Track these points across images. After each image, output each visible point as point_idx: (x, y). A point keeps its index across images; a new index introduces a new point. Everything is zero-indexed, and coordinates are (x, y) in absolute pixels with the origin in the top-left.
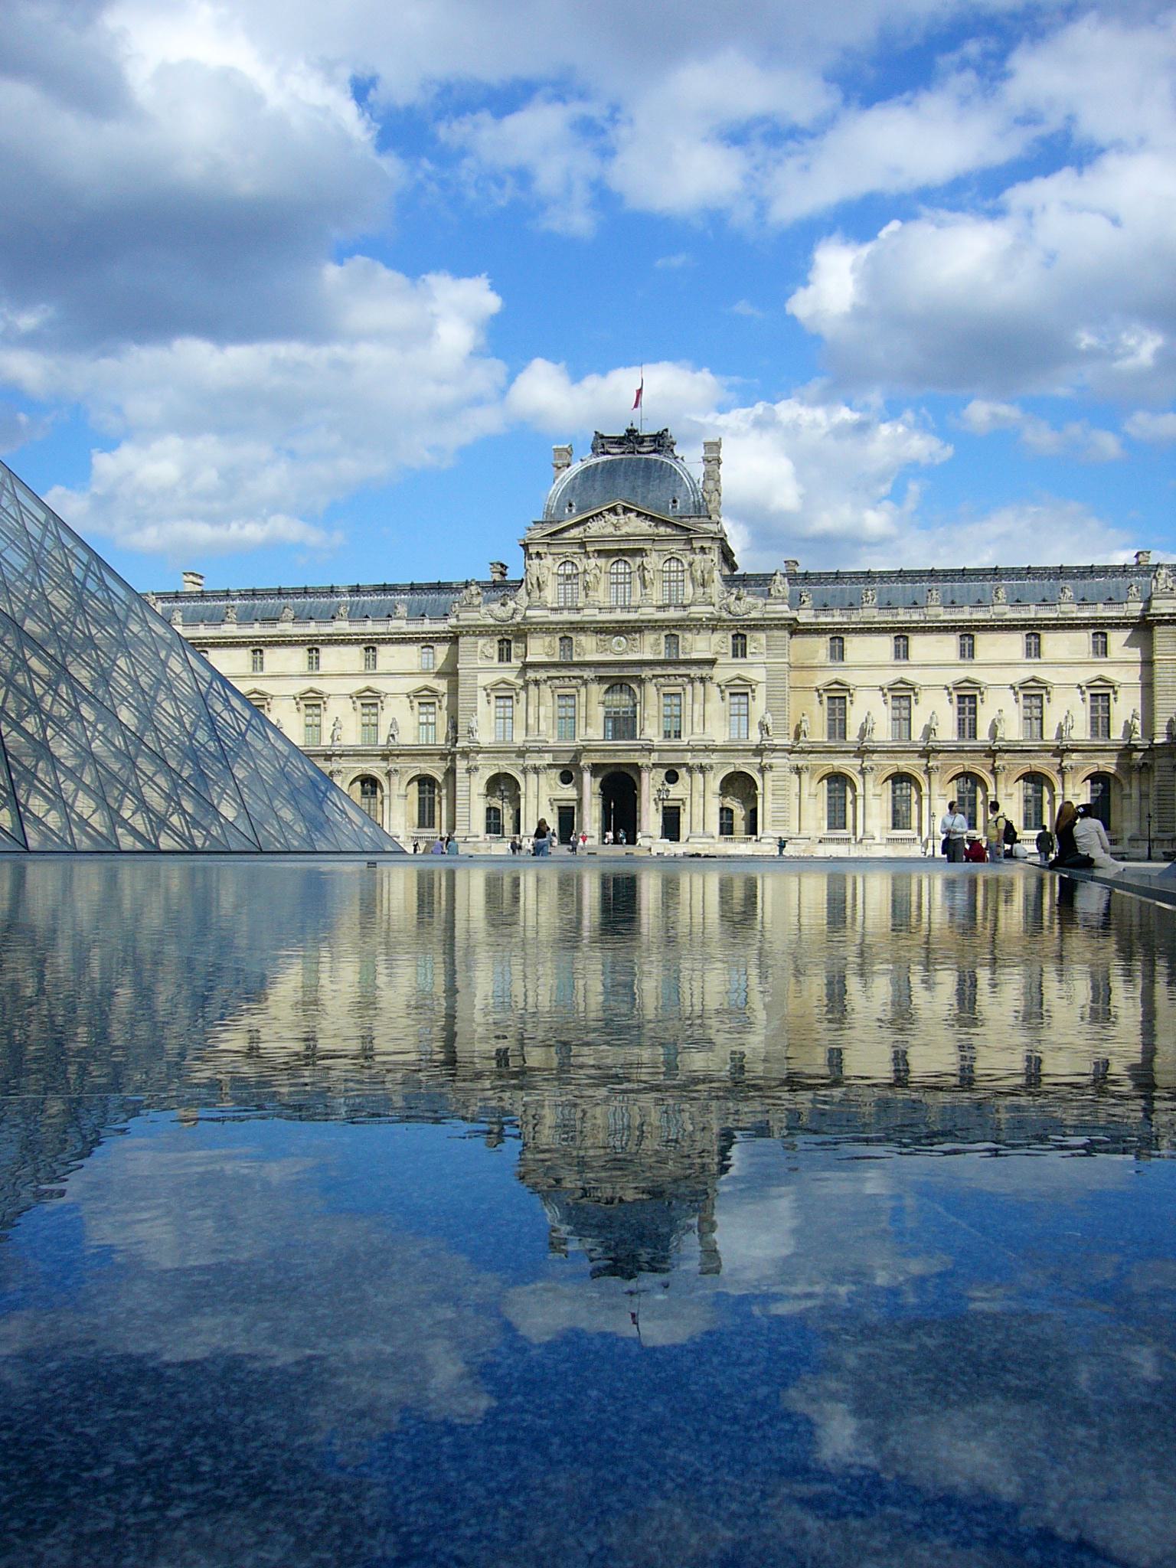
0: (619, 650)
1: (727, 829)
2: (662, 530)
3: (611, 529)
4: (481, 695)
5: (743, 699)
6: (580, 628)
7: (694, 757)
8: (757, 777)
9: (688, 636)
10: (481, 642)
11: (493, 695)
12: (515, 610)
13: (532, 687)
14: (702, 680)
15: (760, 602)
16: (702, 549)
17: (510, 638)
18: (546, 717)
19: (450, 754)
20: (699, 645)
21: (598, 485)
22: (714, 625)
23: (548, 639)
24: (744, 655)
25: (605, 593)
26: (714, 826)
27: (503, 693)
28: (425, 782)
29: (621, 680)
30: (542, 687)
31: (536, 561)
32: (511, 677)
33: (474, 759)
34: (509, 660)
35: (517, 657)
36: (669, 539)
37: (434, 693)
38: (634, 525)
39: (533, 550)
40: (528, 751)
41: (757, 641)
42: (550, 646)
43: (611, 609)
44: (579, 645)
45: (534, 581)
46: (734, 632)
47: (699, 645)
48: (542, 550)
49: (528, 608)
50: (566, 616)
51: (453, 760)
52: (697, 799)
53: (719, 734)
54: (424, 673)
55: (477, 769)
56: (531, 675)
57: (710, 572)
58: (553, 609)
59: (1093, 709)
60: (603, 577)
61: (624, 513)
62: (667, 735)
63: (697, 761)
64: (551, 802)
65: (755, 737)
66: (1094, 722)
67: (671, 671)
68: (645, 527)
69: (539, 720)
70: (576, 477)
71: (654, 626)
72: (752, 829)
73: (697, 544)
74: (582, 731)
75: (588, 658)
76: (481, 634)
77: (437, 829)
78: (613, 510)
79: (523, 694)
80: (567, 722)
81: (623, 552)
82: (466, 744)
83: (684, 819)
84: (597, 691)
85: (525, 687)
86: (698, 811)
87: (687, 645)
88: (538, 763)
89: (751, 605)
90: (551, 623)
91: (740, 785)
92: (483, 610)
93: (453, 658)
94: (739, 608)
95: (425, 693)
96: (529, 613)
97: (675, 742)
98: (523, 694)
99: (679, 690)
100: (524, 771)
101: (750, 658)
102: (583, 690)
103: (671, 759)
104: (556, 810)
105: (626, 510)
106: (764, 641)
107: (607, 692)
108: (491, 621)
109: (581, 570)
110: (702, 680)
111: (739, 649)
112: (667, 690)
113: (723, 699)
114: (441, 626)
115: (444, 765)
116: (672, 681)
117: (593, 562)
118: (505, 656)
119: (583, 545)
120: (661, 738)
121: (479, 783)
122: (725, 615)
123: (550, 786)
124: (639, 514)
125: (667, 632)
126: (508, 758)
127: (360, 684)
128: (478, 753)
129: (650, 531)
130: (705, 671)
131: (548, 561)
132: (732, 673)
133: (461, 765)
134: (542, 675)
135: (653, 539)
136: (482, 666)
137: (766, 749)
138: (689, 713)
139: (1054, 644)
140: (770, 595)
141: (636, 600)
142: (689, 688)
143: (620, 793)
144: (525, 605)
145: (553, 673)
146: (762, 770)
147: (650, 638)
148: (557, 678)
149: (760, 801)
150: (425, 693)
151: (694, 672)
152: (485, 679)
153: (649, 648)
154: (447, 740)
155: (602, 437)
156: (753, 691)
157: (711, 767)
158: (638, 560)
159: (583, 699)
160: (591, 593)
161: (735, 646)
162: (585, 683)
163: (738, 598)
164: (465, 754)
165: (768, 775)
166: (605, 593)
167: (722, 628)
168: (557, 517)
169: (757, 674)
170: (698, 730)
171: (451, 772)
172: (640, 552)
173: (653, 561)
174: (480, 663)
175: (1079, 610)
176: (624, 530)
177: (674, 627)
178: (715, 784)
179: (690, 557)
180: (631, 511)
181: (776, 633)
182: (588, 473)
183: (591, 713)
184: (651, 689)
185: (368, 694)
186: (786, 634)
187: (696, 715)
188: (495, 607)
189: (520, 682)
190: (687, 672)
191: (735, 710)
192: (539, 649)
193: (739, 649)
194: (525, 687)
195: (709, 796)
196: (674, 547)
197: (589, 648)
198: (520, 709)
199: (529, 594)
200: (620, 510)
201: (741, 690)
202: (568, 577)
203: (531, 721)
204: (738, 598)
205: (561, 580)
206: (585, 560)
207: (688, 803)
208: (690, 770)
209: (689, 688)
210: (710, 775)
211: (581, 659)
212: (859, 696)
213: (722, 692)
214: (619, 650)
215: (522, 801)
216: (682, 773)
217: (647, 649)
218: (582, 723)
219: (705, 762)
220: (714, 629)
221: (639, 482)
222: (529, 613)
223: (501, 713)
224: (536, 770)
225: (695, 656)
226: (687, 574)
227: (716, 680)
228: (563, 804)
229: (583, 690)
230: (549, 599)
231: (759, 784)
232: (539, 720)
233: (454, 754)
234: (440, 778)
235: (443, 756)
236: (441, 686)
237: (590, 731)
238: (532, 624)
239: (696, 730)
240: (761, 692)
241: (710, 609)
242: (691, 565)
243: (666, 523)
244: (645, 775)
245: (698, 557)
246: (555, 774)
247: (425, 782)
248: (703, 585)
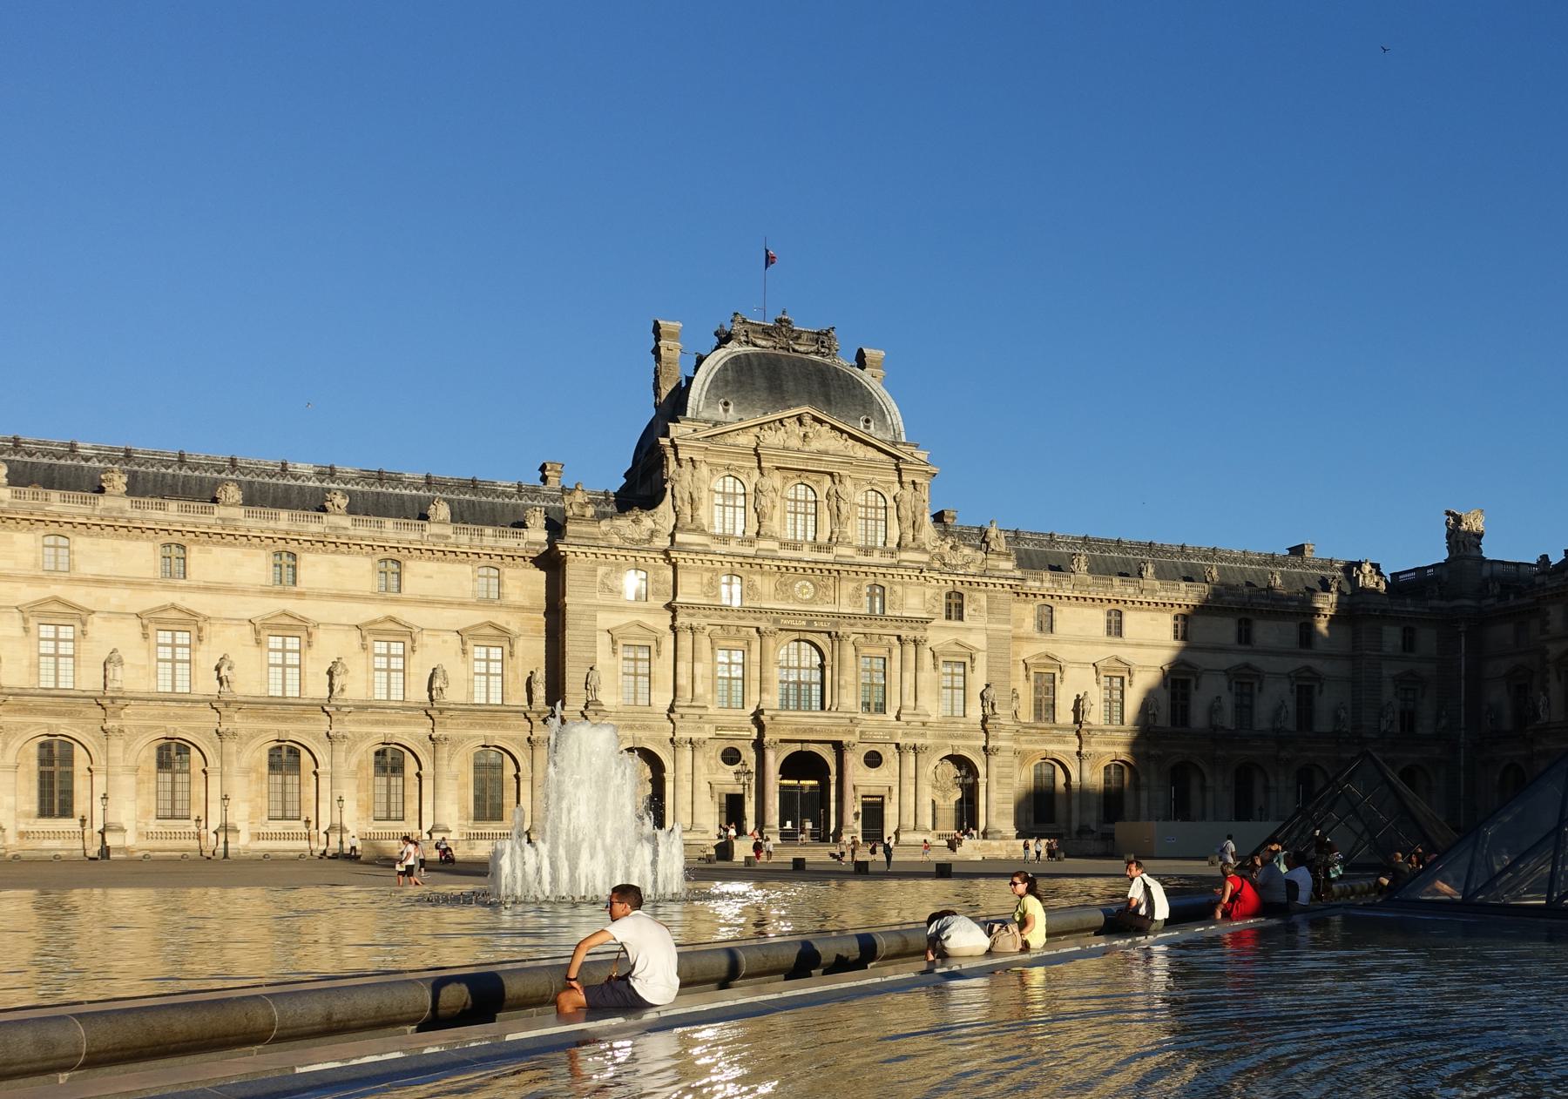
11: (620, 643)
24: (961, 618)
36: (869, 465)
41: (976, 603)
106: (984, 603)
147: (848, 587)
153: (847, 600)
212: (1070, 673)
226: (892, 513)
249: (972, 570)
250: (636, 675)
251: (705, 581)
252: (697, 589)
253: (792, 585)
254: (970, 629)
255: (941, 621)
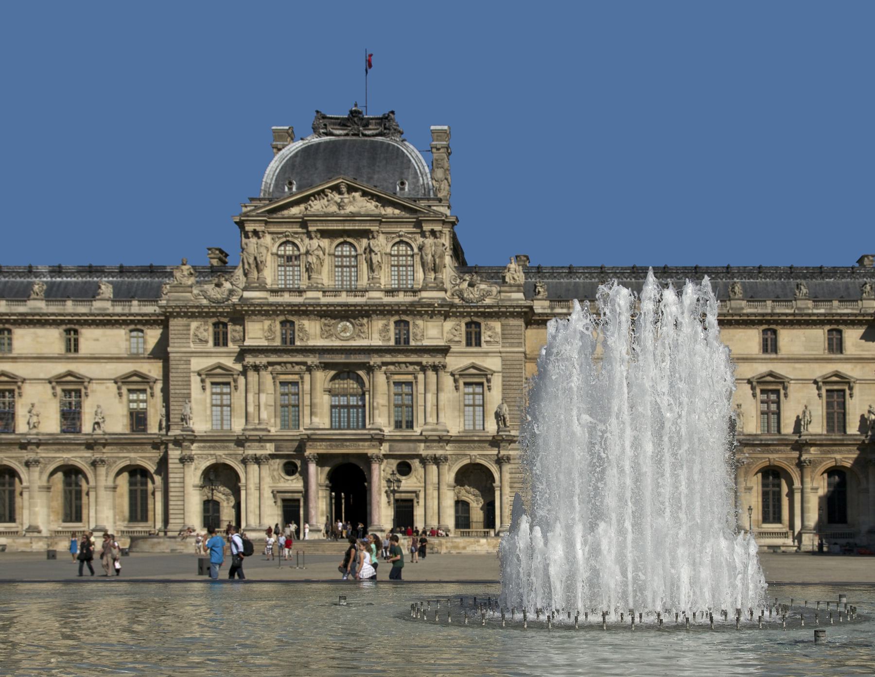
0: (346, 335)
1: (463, 521)
2: (390, 211)
3: (334, 209)
4: (195, 381)
5: (478, 390)
6: (303, 311)
7: (427, 448)
8: (494, 469)
9: (420, 322)
10: (194, 325)
12: (231, 292)
13: (252, 376)
14: (435, 368)
15: (495, 289)
16: (433, 233)
17: (225, 320)
18: (267, 405)
19: (162, 443)
20: (432, 332)
21: (320, 164)
22: (445, 311)
23: (267, 323)
24: (479, 344)
25: (328, 273)
26: (449, 521)
27: (218, 378)
28: (137, 473)
29: (348, 367)
30: (263, 373)
31: (253, 240)
32: (229, 362)
33: (189, 448)
34: (225, 344)
35: (234, 341)
37: (145, 379)
38: (359, 204)
39: (249, 227)
40: (247, 440)
42: (270, 330)
43: (336, 292)
44: (302, 329)
45: (251, 260)
46: (468, 319)
47: (432, 332)
48: (260, 228)
49: (245, 289)
50: (287, 298)
51: (166, 448)
52: (433, 493)
53: (453, 425)
54: (134, 357)
55: (191, 459)
56: (250, 360)
57: (442, 257)
58: (274, 292)
59: (829, 405)
60: (327, 260)
61: (349, 192)
62: (398, 425)
63: (430, 452)
64: (275, 493)
65: (492, 427)
66: (830, 417)
67: (401, 358)
68: (370, 206)
69: (258, 404)
70: (296, 155)
71: (382, 311)
72: (489, 522)
73: (427, 227)
74: (307, 420)
75: (311, 343)
76: (193, 316)
77: (150, 523)
78: (336, 189)
79: (241, 380)
80: (290, 410)
81: (349, 233)
82: (178, 432)
83: (419, 512)
84: (322, 378)
85: (244, 373)
86: (433, 504)
87: (418, 331)
88: (259, 453)
89: (485, 293)
90: (271, 305)
91: (475, 476)
92: (195, 291)
93: (163, 343)
94: (472, 294)
95: (135, 379)
96: (247, 294)
97: (407, 433)
98: (241, 380)
99: (410, 378)
100: (244, 462)
101: (485, 347)
102: (307, 377)
103: (404, 449)
104: (279, 503)
105: (351, 189)
107: (333, 379)
108: (205, 302)
109: (303, 250)
110: (435, 368)
111: (473, 338)
112: (397, 378)
113: (457, 388)
114: (150, 309)
115: (157, 455)
116: (403, 368)
117: (315, 243)
118: (220, 340)
119: (304, 224)
120: (392, 428)
121: (193, 475)
122: (457, 301)
123: (273, 477)
124: (365, 194)
125: (397, 318)
126: (224, 448)
127: (60, 368)
128: (192, 442)
129: (377, 212)
130: (437, 360)
131: (267, 239)
132: (465, 362)
133: (174, 454)
134: (262, 360)
135: (380, 220)
136: (197, 350)
137: (503, 440)
138: (421, 401)
139: (791, 340)
140: (504, 282)
141: (364, 282)
142: (421, 376)
143: (349, 483)
144: (242, 286)
145: (273, 359)
146: (500, 461)
147: (378, 324)
148: (279, 363)
149: (497, 493)
150: (135, 379)
151: (426, 360)
152: (198, 364)
153: (377, 334)
154: (160, 429)
155: (324, 117)
156: (489, 381)
157: (446, 459)
158: (365, 242)
159: (307, 387)
160: (314, 276)
161: (468, 334)
162: (309, 369)
163: (471, 285)
164: (178, 443)
165: (506, 468)
166: (328, 273)
167: (455, 315)
168: (277, 194)
169: (493, 363)
170: (432, 419)
171: (163, 465)
172: (366, 234)
173: (381, 244)
174: (193, 347)
175: (816, 307)
176: (350, 209)
177: (405, 312)
178: (449, 476)
179: (420, 240)
180: (356, 190)
181: (513, 322)
182: (308, 152)
183: (317, 400)
184: (380, 378)
185: (70, 378)
186: (520, 322)
187: (429, 405)
188: (210, 288)
189: (239, 367)
190: (419, 360)
191: (469, 400)
192: (257, 333)
193: (473, 338)
194: (244, 373)
195: (444, 488)
196: (403, 230)
197: (312, 334)
198: (238, 398)
199: (246, 275)
200: (344, 190)
201: (476, 379)
202: (289, 258)
203: (251, 409)
204: (471, 285)
205: (282, 261)
206: (307, 241)
207: (422, 495)
208: (424, 461)
209: (421, 376)
210: (445, 468)
211: (303, 344)
213: (456, 381)
214: (346, 335)
215: (243, 493)
216: (416, 464)
217: (376, 336)
218: (307, 411)
219: (439, 452)
220: (446, 316)
221: (364, 162)
222: (247, 294)
223: (217, 399)
224: (257, 460)
225: (426, 343)
226: (417, 259)
227: (450, 369)
228: (288, 496)
229: (307, 377)
230: (269, 281)
231: (497, 476)
232: (258, 404)
233: (166, 444)
234: (152, 468)
235: (156, 446)
236: (153, 369)
237: (316, 420)
238: (252, 305)
239: (429, 420)
240: (497, 382)
241: (441, 294)
242: (421, 248)
243: (395, 205)
244: (375, 467)
245: (430, 241)
246: (278, 464)
247: (137, 473)
248: (435, 269)
249: (488, 301)
250: (222, 406)
251: (266, 327)
252: (259, 334)
253: (336, 325)
254: (486, 353)
255: (462, 348)
